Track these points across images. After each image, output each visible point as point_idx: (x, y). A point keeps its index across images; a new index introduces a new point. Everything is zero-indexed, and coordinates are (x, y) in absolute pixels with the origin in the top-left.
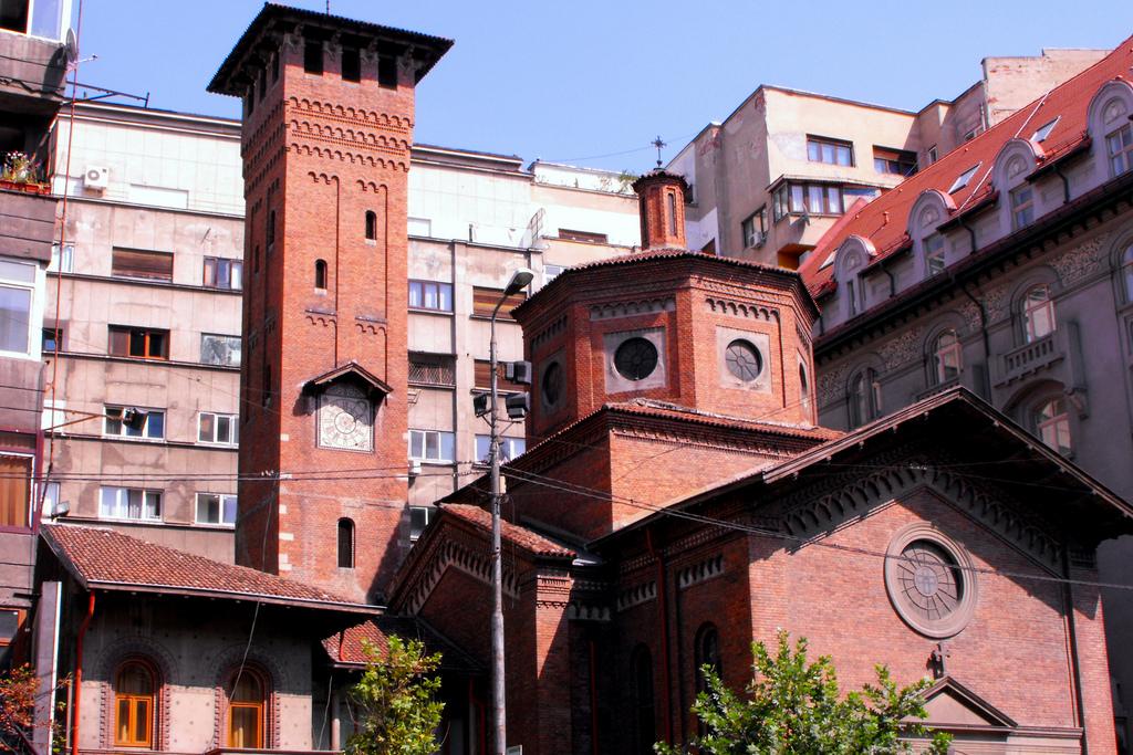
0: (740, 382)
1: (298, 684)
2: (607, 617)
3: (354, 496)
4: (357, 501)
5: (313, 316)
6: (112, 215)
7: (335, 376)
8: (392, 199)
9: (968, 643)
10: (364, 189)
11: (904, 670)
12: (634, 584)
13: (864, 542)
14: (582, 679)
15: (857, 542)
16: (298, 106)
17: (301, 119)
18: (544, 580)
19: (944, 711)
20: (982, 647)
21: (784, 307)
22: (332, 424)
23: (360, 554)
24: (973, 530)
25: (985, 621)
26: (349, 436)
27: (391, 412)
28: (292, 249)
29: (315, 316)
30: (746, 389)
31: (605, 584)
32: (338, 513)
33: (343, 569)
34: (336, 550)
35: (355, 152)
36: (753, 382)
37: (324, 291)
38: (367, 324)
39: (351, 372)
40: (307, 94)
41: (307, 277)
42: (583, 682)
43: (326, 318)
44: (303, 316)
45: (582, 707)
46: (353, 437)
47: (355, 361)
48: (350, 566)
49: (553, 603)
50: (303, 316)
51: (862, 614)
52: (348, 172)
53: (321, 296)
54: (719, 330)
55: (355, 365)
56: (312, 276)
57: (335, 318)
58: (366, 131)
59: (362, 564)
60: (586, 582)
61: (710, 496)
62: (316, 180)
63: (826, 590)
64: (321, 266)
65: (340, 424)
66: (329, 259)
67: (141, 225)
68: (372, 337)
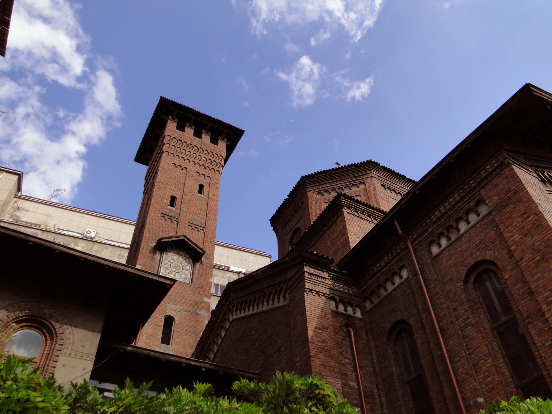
1: (83, 346)
2: (359, 314)
3: (176, 304)
4: (178, 308)
5: (166, 216)
6: (93, 246)
7: (173, 239)
8: (212, 182)
10: (200, 175)
12: (382, 279)
14: (346, 358)
16: (171, 139)
17: (172, 144)
18: (310, 274)
22: (170, 270)
23: (176, 338)
26: (177, 274)
27: (203, 267)
28: (159, 188)
29: (167, 217)
31: (355, 290)
32: (165, 312)
33: (164, 345)
34: (161, 333)
35: (196, 161)
37: (174, 209)
38: (195, 226)
39: (183, 239)
40: (176, 136)
41: (165, 201)
42: (349, 361)
43: (173, 219)
44: (160, 215)
45: (350, 383)
46: (180, 275)
47: (185, 234)
48: (169, 344)
49: (318, 292)
50: (160, 215)
52: (192, 168)
53: (172, 210)
54: (390, 199)
55: (185, 236)
57: (177, 220)
58: (203, 156)
59: (176, 344)
60: (341, 286)
61: (464, 146)
62: (176, 167)
64: (173, 199)
65: (173, 267)
66: (177, 194)
67: (105, 250)
68: (196, 232)
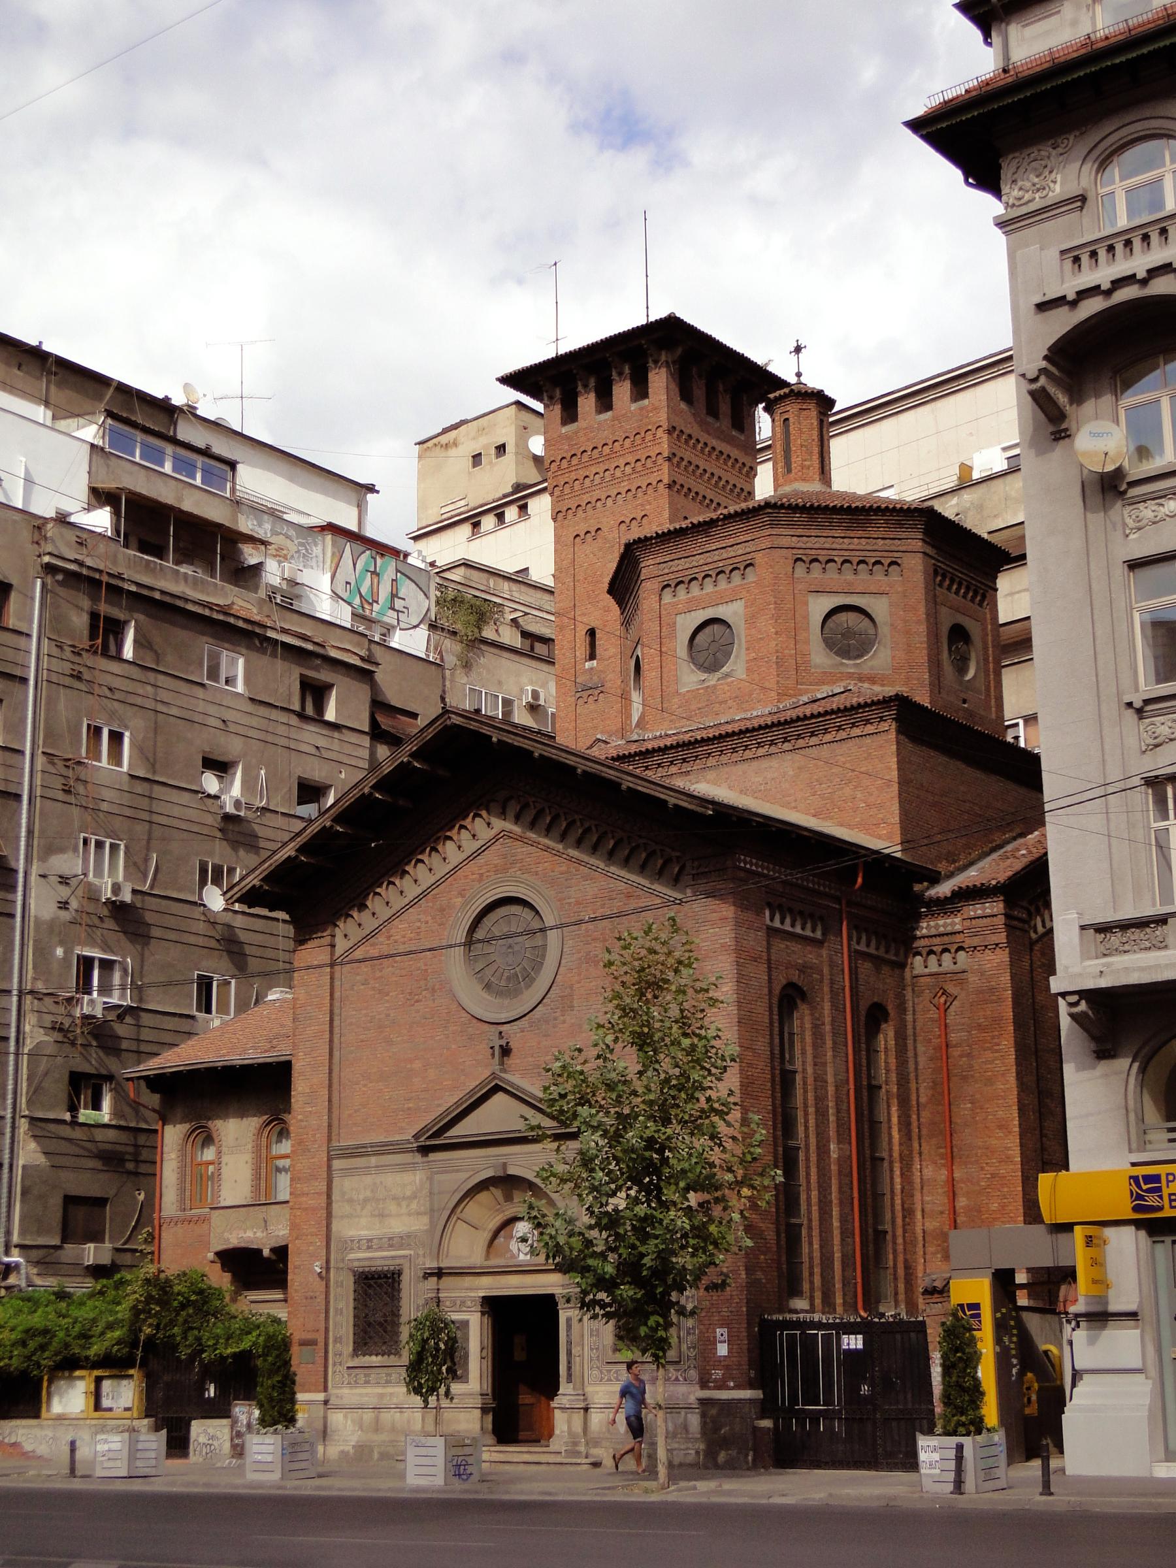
0: (704, 676)
9: (547, 1022)
11: (463, 1070)
13: (427, 922)
15: (418, 924)
19: (498, 1115)
20: (564, 1022)
21: (760, 554)
24: (564, 868)
25: (571, 987)
30: (712, 683)
36: (725, 669)
51: (417, 1011)
54: (680, 619)
56: (582, 649)
63: (380, 992)
64: (592, 633)
